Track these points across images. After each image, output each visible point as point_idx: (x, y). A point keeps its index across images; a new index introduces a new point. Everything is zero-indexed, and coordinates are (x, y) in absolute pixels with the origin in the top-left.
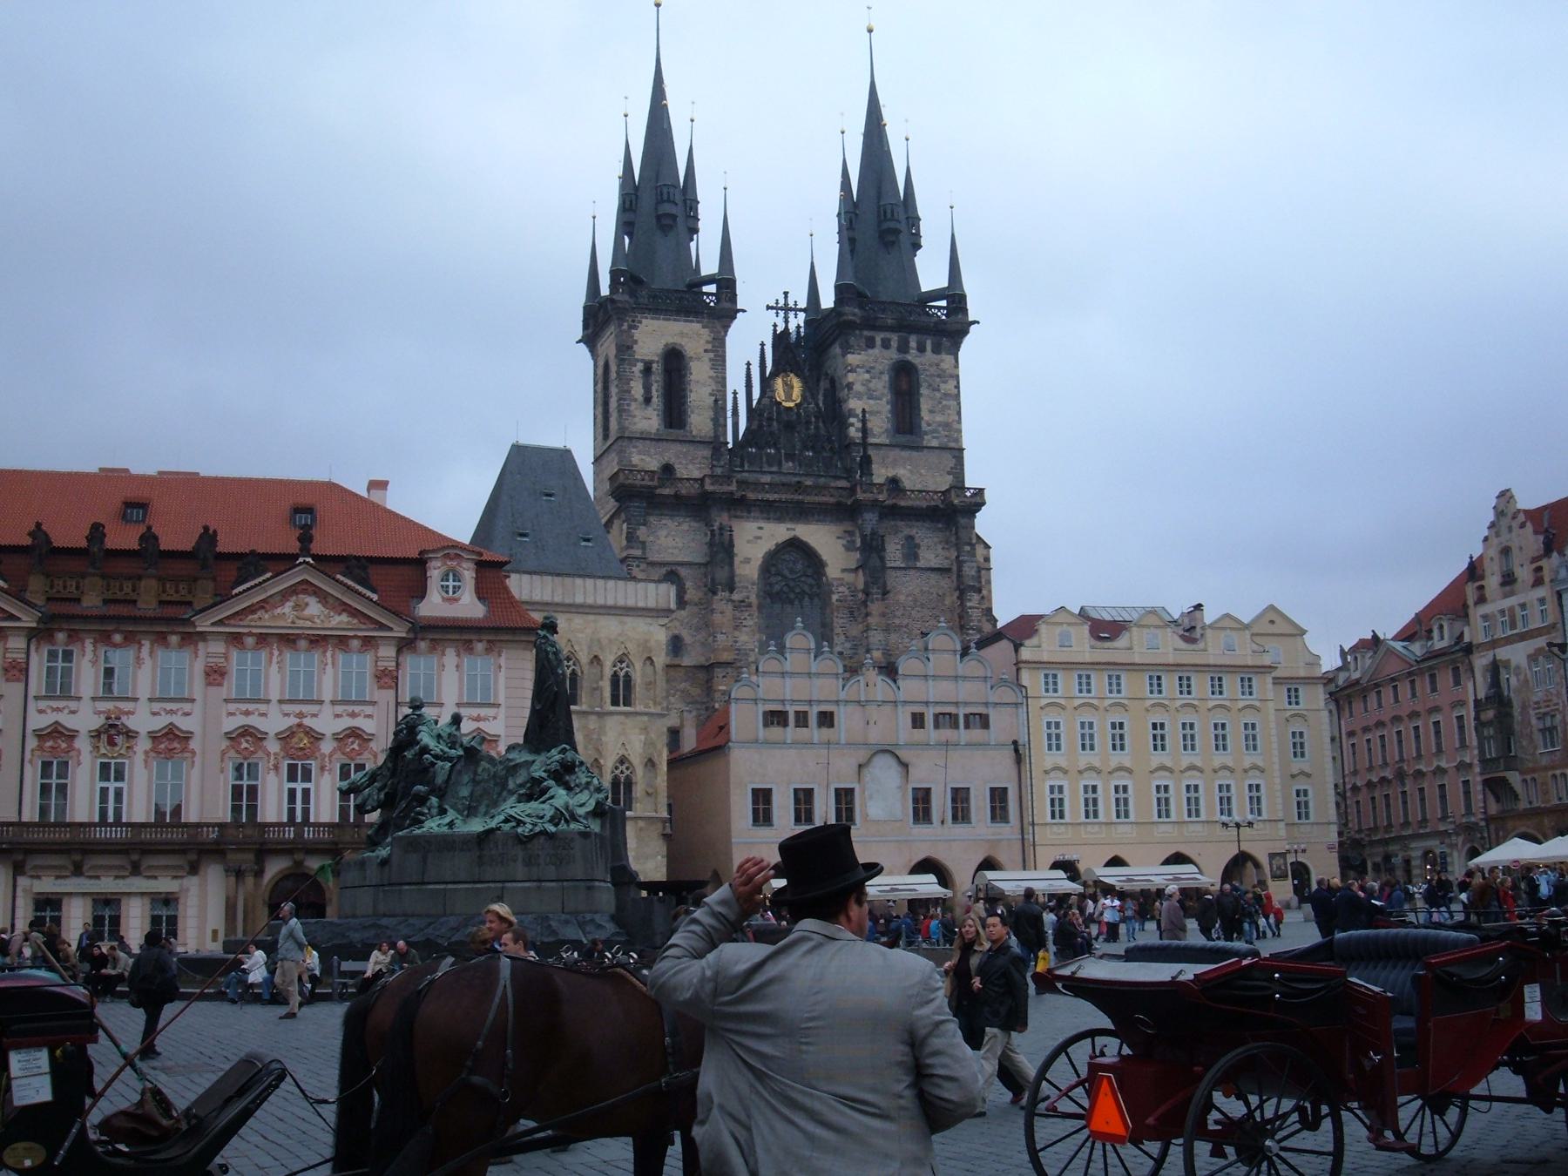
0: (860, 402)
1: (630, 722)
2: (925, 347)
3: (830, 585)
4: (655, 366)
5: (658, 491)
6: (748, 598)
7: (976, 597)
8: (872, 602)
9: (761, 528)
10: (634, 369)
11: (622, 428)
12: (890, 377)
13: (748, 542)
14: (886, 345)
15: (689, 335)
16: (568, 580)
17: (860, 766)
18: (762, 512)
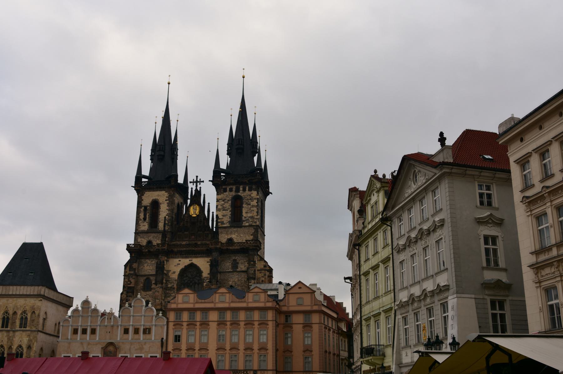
0: (219, 212)
1: (24, 333)
2: (246, 189)
3: (204, 279)
4: (148, 207)
5: (144, 251)
6: (173, 286)
7: (253, 281)
8: (212, 285)
9: (180, 261)
10: (141, 209)
11: (136, 230)
12: (232, 203)
13: (175, 266)
14: (231, 190)
15: (162, 196)
16: (8, 287)
17: (102, 348)
18: (181, 255)
